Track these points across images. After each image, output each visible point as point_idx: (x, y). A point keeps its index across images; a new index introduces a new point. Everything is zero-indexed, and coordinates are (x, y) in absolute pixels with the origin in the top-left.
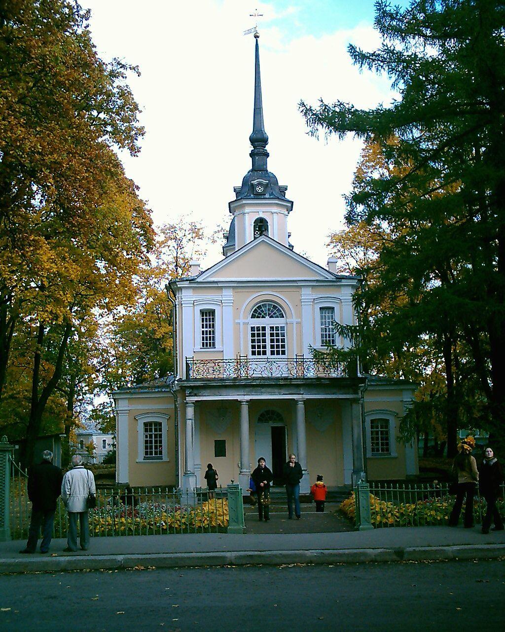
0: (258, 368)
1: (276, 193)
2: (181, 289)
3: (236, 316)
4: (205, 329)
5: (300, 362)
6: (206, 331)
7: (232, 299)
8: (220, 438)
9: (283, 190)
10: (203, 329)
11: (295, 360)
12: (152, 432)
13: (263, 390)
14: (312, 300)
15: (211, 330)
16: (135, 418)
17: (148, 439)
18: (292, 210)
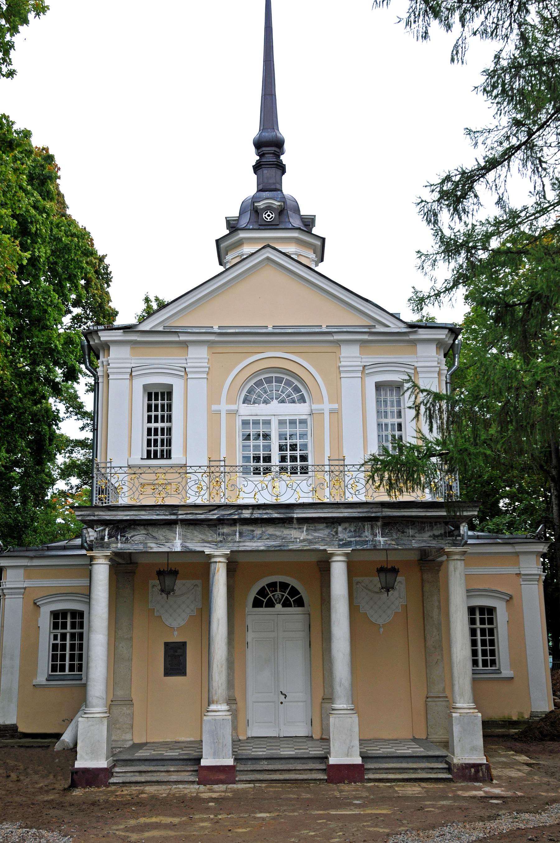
0: (254, 491)
1: (296, 223)
2: (106, 346)
3: (213, 397)
4: (153, 425)
5: (337, 473)
6: (156, 429)
7: (206, 365)
8: (176, 638)
9: (308, 223)
10: (150, 425)
11: (327, 468)
12: (66, 628)
13: (258, 531)
14: (361, 368)
15: (165, 425)
16: (35, 604)
17: (58, 642)
18: (322, 260)
